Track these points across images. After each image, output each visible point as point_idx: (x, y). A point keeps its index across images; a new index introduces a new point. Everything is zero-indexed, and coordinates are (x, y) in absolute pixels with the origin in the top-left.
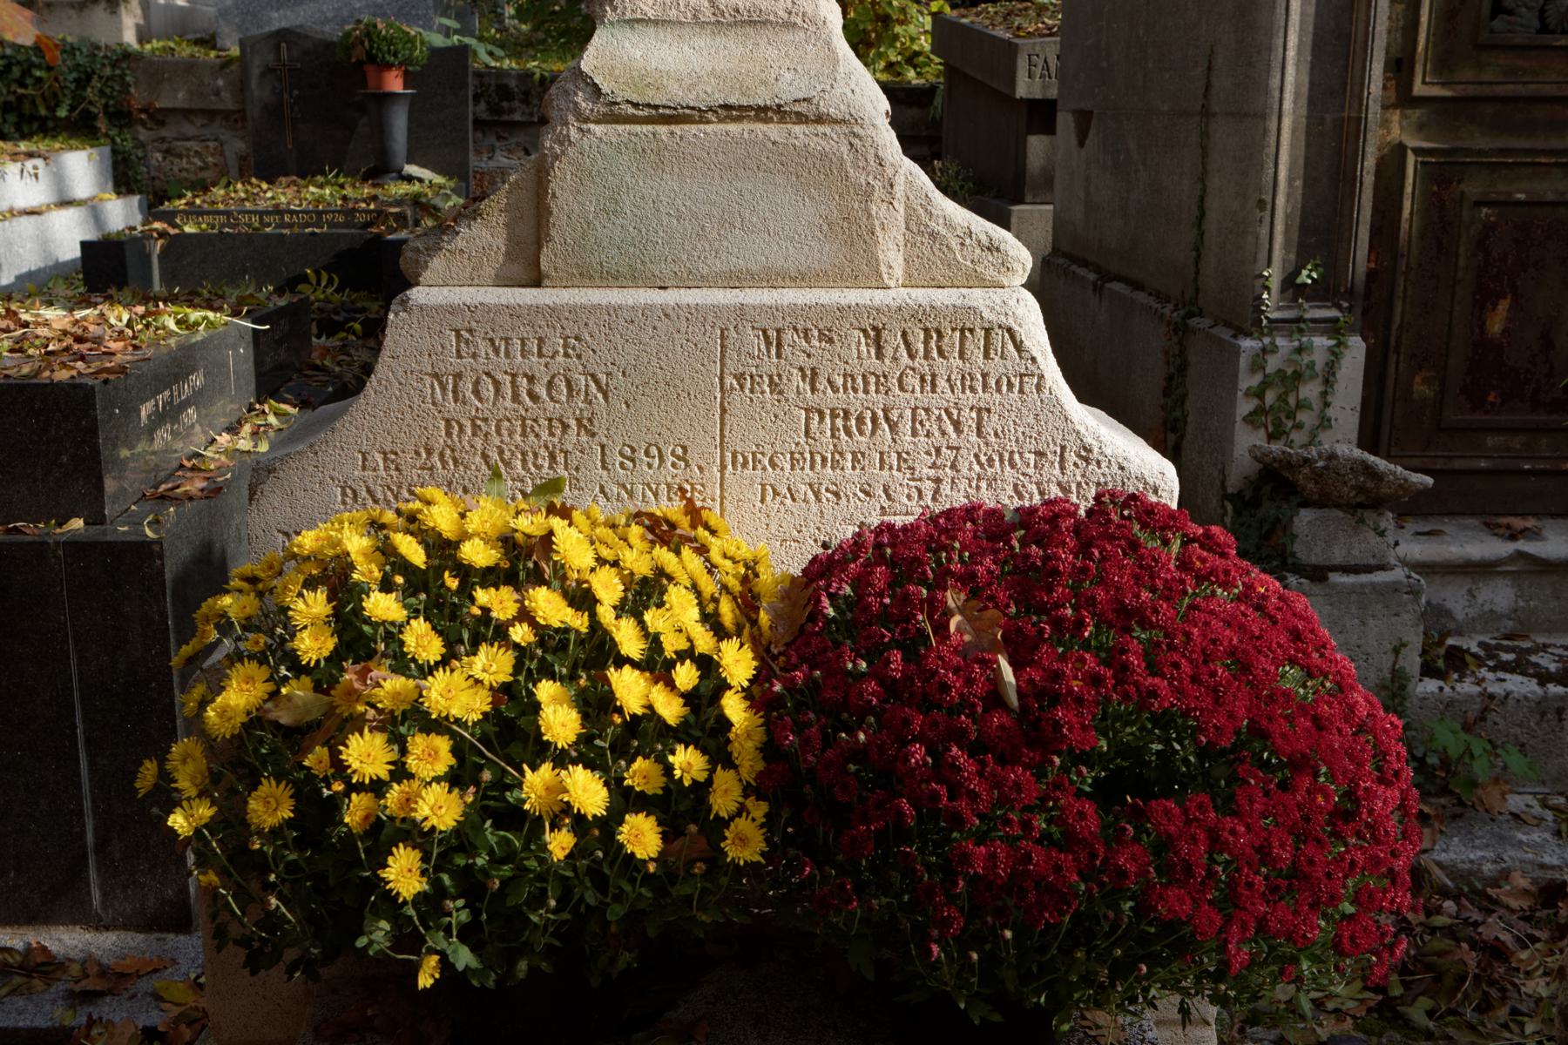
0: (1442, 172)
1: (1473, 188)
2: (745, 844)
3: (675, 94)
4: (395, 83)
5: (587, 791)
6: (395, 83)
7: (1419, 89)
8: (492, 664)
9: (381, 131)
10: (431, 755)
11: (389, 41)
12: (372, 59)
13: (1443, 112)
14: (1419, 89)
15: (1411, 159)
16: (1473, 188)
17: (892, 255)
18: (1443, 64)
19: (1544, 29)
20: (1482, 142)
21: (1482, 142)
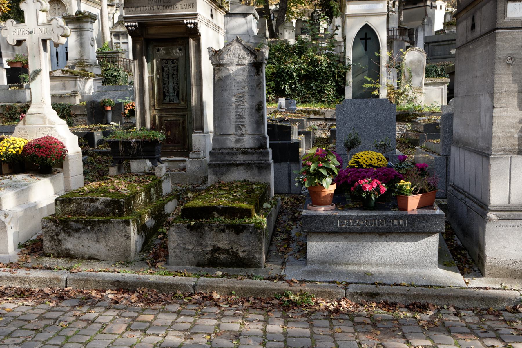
0: (160, 117)
1: (164, 119)
2: (20, 153)
3: (33, 113)
4: (109, 109)
5: (12, 150)
6: (109, 109)
7: (156, 108)
8: (9, 144)
9: (107, 117)
10: (5, 148)
11: (107, 102)
12: (104, 105)
13: (160, 110)
14: (156, 108)
15: (156, 116)
16: (164, 119)
17: (47, 122)
18: (159, 105)
19: (170, 101)
20: (164, 114)
21: (164, 114)
